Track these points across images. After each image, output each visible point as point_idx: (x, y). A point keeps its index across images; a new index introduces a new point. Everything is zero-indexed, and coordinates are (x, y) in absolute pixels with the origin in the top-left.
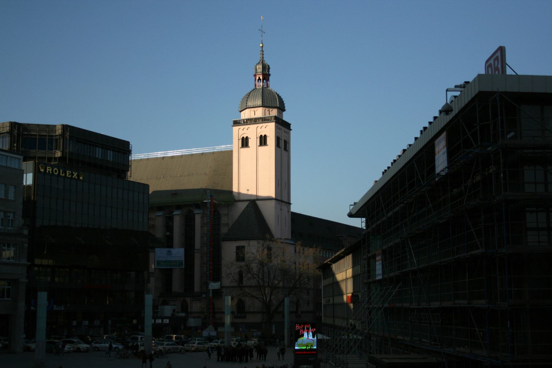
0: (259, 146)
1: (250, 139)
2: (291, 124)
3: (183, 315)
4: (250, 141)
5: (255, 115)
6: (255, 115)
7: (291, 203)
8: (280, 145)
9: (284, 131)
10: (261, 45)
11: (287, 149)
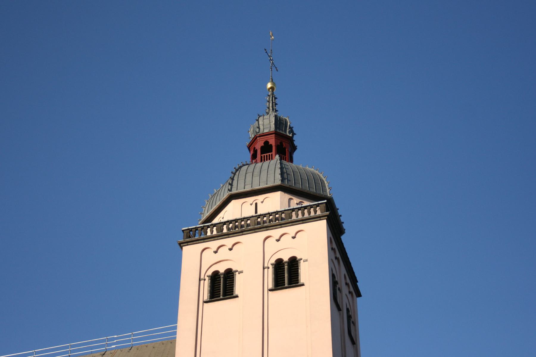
1: (241, 272)
4: (239, 280)
10: (269, 85)
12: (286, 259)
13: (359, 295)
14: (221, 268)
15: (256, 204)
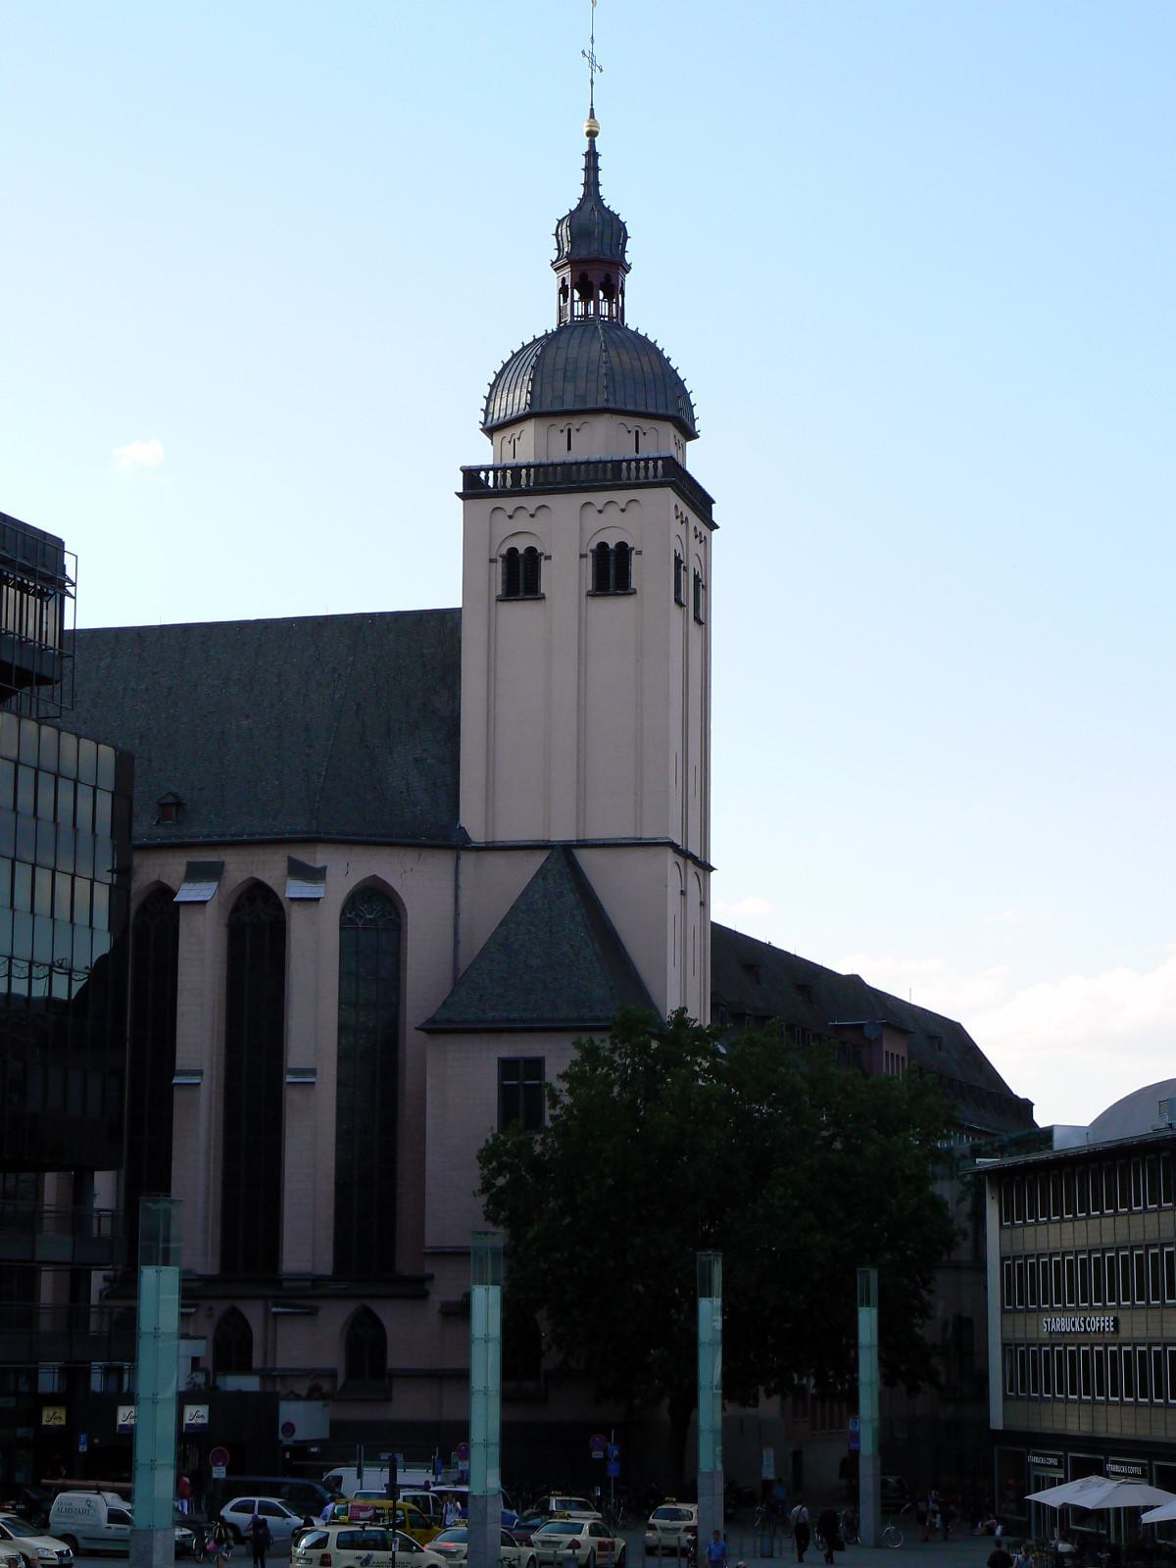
0: (592, 596)
1: (549, 558)
2: (714, 502)
5: (569, 448)
6: (569, 448)
7: (713, 864)
13: (713, 526)
15: (569, 430)
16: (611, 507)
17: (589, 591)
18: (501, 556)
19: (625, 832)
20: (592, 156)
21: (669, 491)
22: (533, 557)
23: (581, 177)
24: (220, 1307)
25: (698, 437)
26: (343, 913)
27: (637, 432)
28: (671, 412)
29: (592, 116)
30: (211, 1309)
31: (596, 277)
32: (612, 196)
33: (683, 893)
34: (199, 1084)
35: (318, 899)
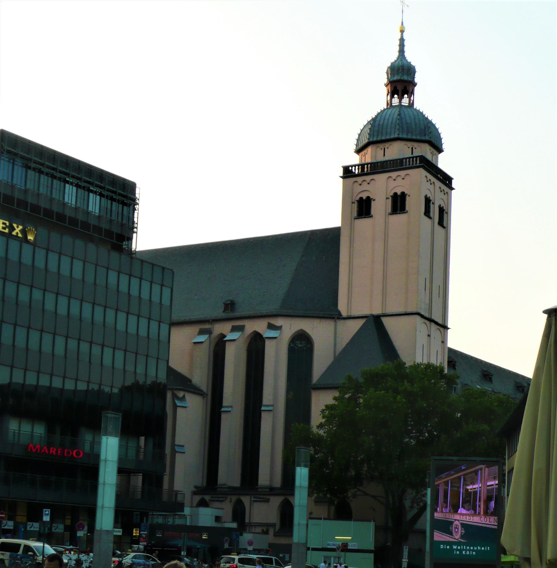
1: (374, 200)
3: (234, 525)
5: (384, 155)
6: (384, 155)
7: (449, 327)
8: (431, 215)
9: (440, 188)
11: (445, 225)
12: (399, 193)
14: (364, 196)
15: (384, 148)
16: (399, 178)
17: (389, 213)
18: (356, 201)
19: (401, 310)
20: (402, 40)
21: (421, 170)
22: (369, 200)
23: (397, 48)
24: (234, 498)
25: (443, 151)
26: (290, 345)
27: (412, 148)
28: (427, 138)
29: (402, 24)
30: (231, 499)
31: (400, 88)
32: (411, 57)
33: (429, 336)
34: (230, 411)
35: (275, 338)
